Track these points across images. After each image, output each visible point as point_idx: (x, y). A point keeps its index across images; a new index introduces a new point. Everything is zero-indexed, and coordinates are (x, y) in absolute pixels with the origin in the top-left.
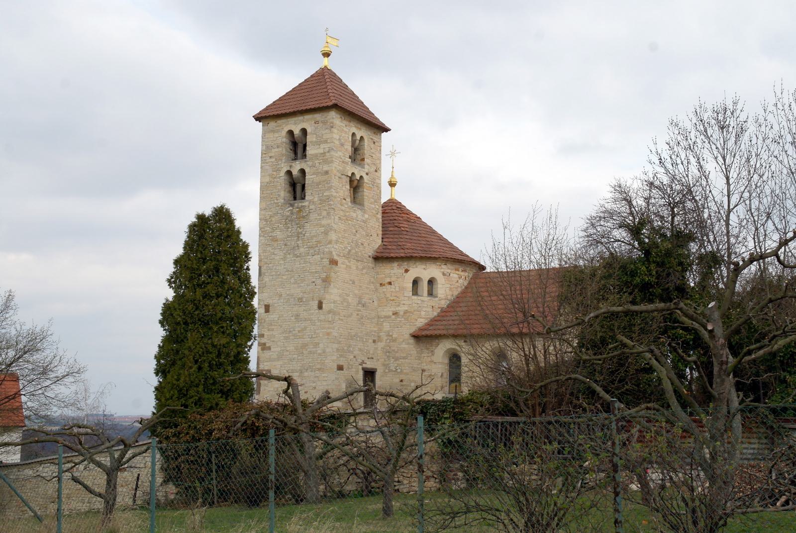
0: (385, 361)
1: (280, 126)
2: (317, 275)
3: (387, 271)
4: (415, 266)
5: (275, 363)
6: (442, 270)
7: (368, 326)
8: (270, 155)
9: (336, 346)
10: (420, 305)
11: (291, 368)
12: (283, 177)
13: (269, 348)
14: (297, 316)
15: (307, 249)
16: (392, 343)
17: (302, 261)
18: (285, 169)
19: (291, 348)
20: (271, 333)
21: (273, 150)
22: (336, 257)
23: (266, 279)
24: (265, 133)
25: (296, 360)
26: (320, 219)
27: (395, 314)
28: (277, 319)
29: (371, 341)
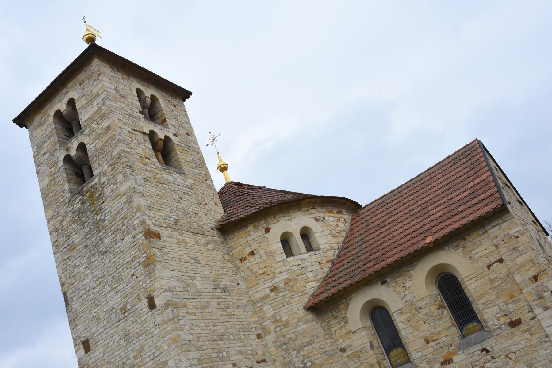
0: (284, 358)
2: (134, 263)
3: (243, 241)
4: (275, 221)
6: (313, 216)
7: (243, 317)
8: (43, 152)
9: (193, 355)
10: (303, 266)
12: (63, 167)
15: (113, 236)
16: (284, 330)
17: (111, 256)
18: (62, 157)
22: (153, 228)
23: (76, 306)
24: (32, 133)
27: (274, 289)
28: (102, 354)
29: (253, 337)
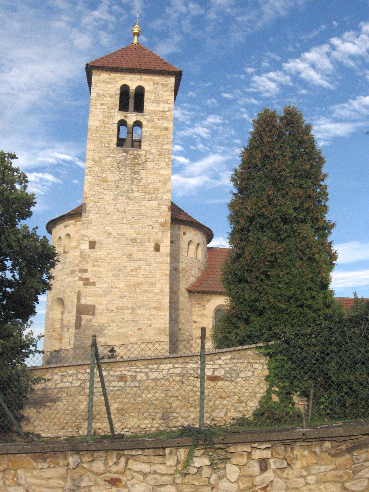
1: (114, 79)
5: (99, 299)
11: (121, 305)
13: (94, 284)
14: (130, 255)
15: (143, 194)
19: (122, 286)
20: (96, 269)
21: (105, 99)
25: (128, 298)
26: (158, 169)
28: (104, 256)
